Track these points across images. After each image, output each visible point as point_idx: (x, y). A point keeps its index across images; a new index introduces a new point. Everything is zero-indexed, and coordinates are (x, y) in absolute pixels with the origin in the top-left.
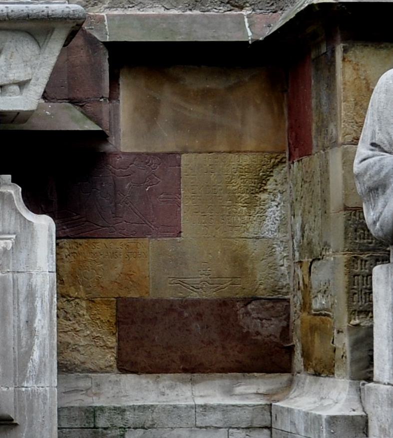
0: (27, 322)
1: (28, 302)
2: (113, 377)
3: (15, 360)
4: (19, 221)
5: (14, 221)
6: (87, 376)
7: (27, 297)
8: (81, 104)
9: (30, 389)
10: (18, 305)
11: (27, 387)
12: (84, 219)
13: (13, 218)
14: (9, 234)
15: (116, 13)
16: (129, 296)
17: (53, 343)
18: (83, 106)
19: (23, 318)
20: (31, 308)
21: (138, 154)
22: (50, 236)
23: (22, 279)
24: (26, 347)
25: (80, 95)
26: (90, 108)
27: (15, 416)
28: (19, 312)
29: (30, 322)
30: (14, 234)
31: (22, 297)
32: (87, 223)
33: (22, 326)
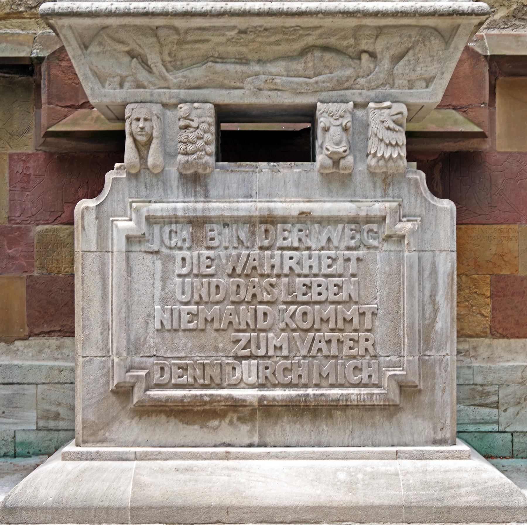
0: (431, 296)
1: (431, 278)
2: (487, 341)
3: (419, 331)
4: (424, 204)
5: (419, 204)
6: (465, 341)
7: (431, 274)
8: (463, 110)
9: (432, 357)
10: (423, 281)
11: (429, 356)
12: (464, 208)
13: (419, 202)
14: (415, 216)
15: (493, 32)
16: (502, 273)
17: (453, 316)
18: (465, 111)
19: (427, 293)
20: (434, 284)
21: (511, 154)
22: (452, 218)
23: (427, 256)
24: (429, 319)
25: (462, 103)
26: (471, 114)
27: (419, 383)
28: (424, 288)
29: (433, 296)
30: (420, 216)
31: (427, 274)
32: (467, 211)
33: (426, 299)
